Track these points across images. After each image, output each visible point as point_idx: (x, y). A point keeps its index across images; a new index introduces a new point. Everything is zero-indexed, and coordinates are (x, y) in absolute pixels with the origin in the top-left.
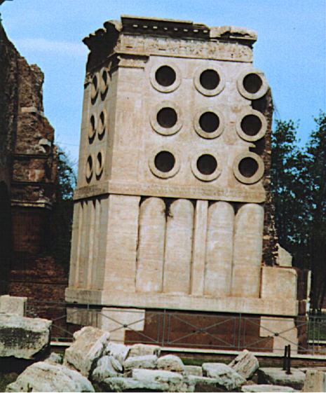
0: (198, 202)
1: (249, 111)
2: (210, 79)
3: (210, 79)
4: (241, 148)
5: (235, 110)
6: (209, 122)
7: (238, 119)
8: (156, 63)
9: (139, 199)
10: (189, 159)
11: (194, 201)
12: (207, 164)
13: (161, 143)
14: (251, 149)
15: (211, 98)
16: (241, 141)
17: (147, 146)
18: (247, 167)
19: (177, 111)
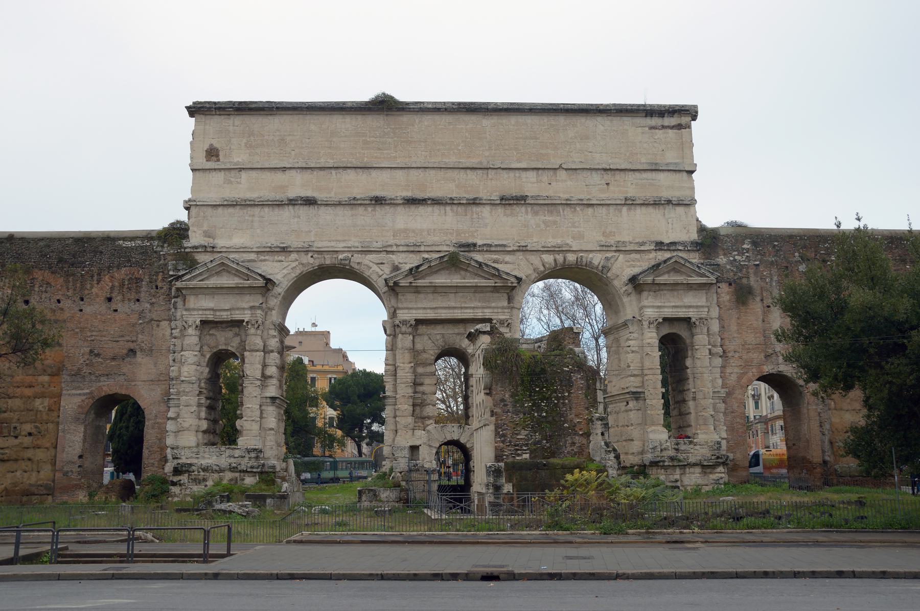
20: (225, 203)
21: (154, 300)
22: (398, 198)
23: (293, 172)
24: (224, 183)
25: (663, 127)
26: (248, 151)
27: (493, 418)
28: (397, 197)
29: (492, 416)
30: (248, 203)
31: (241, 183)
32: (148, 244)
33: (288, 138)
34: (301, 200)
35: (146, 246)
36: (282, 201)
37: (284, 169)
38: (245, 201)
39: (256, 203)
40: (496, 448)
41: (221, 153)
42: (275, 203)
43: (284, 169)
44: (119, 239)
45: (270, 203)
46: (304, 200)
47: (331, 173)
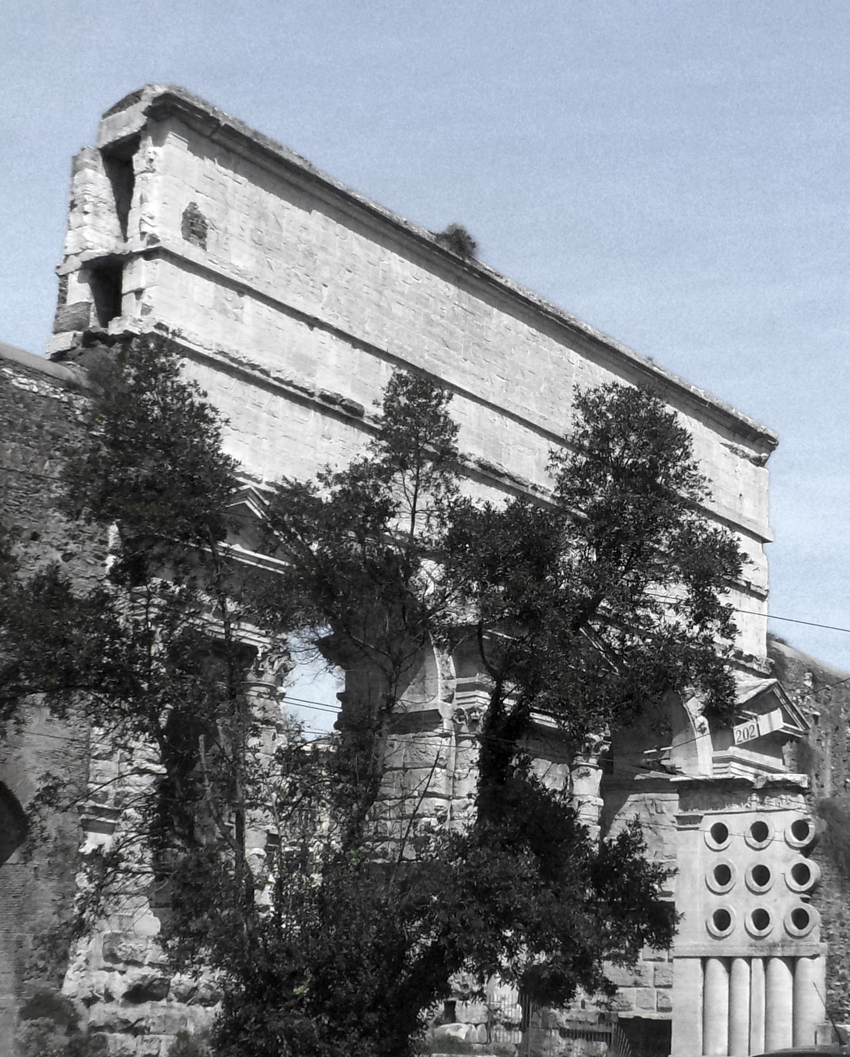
0: (753, 961)
1: (800, 859)
2: (760, 831)
3: (760, 831)
4: (794, 902)
5: (786, 860)
6: (762, 875)
7: (788, 869)
8: (709, 822)
9: (699, 961)
10: (745, 915)
11: (749, 959)
12: (761, 918)
13: (716, 903)
14: (805, 900)
15: (761, 852)
16: (791, 893)
17: (706, 906)
18: (800, 918)
19: (730, 867)
20: (219, 358)
21: (72, 547)
22: (472, 458)
23: (326, 336)
24: (214, 308)
25: (745, 456)
26: (253, 251)
27: (825, 945)
28: (471, 455)
29: (822, 941)
30: (257, 373)
31: (238, 319)
32: (65, 399)
33: (321, 255)
34: (345, 407)
35: (59, 401)
36: (312, 395)
37: (313, 322)
38: (254, 367)
39: (271, 381)
40: (829, 997)
41: (210, 232)
42: (299, 393)
43: (313, 322)
44: (14, 364)
45: (291, 389)
46: (345, 407)
47: (380, 363)
